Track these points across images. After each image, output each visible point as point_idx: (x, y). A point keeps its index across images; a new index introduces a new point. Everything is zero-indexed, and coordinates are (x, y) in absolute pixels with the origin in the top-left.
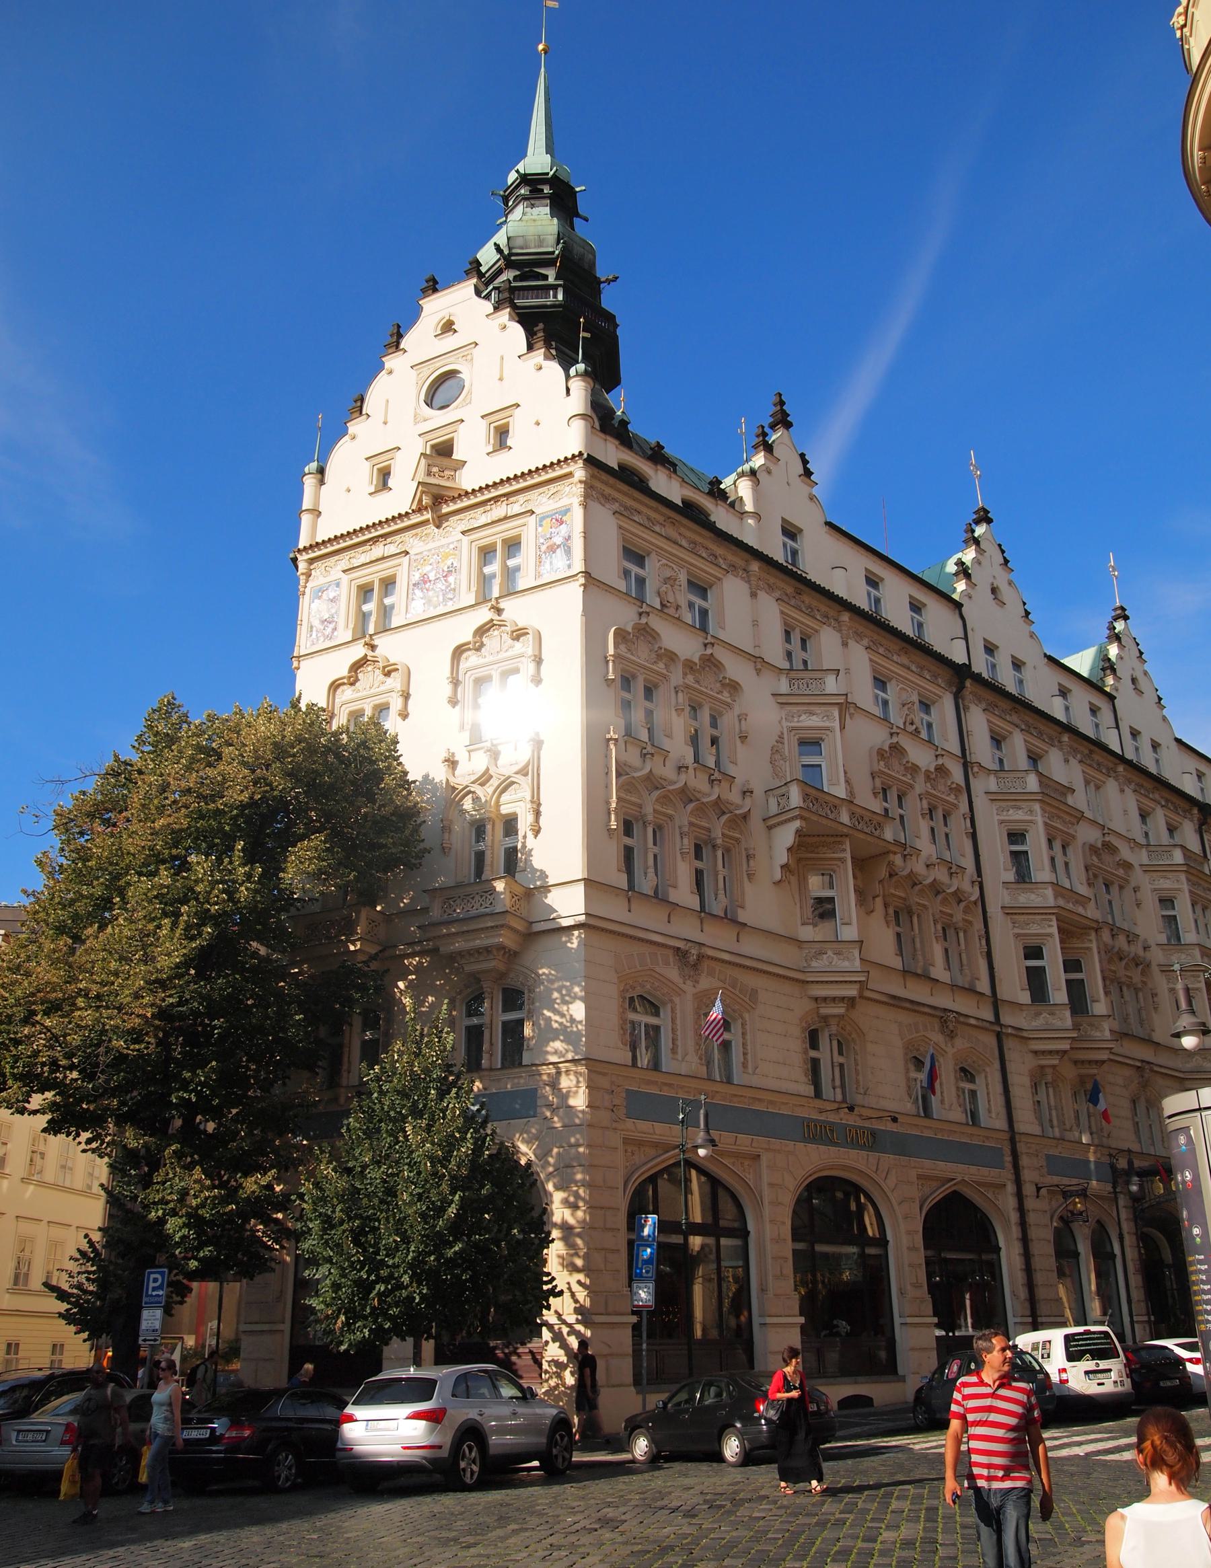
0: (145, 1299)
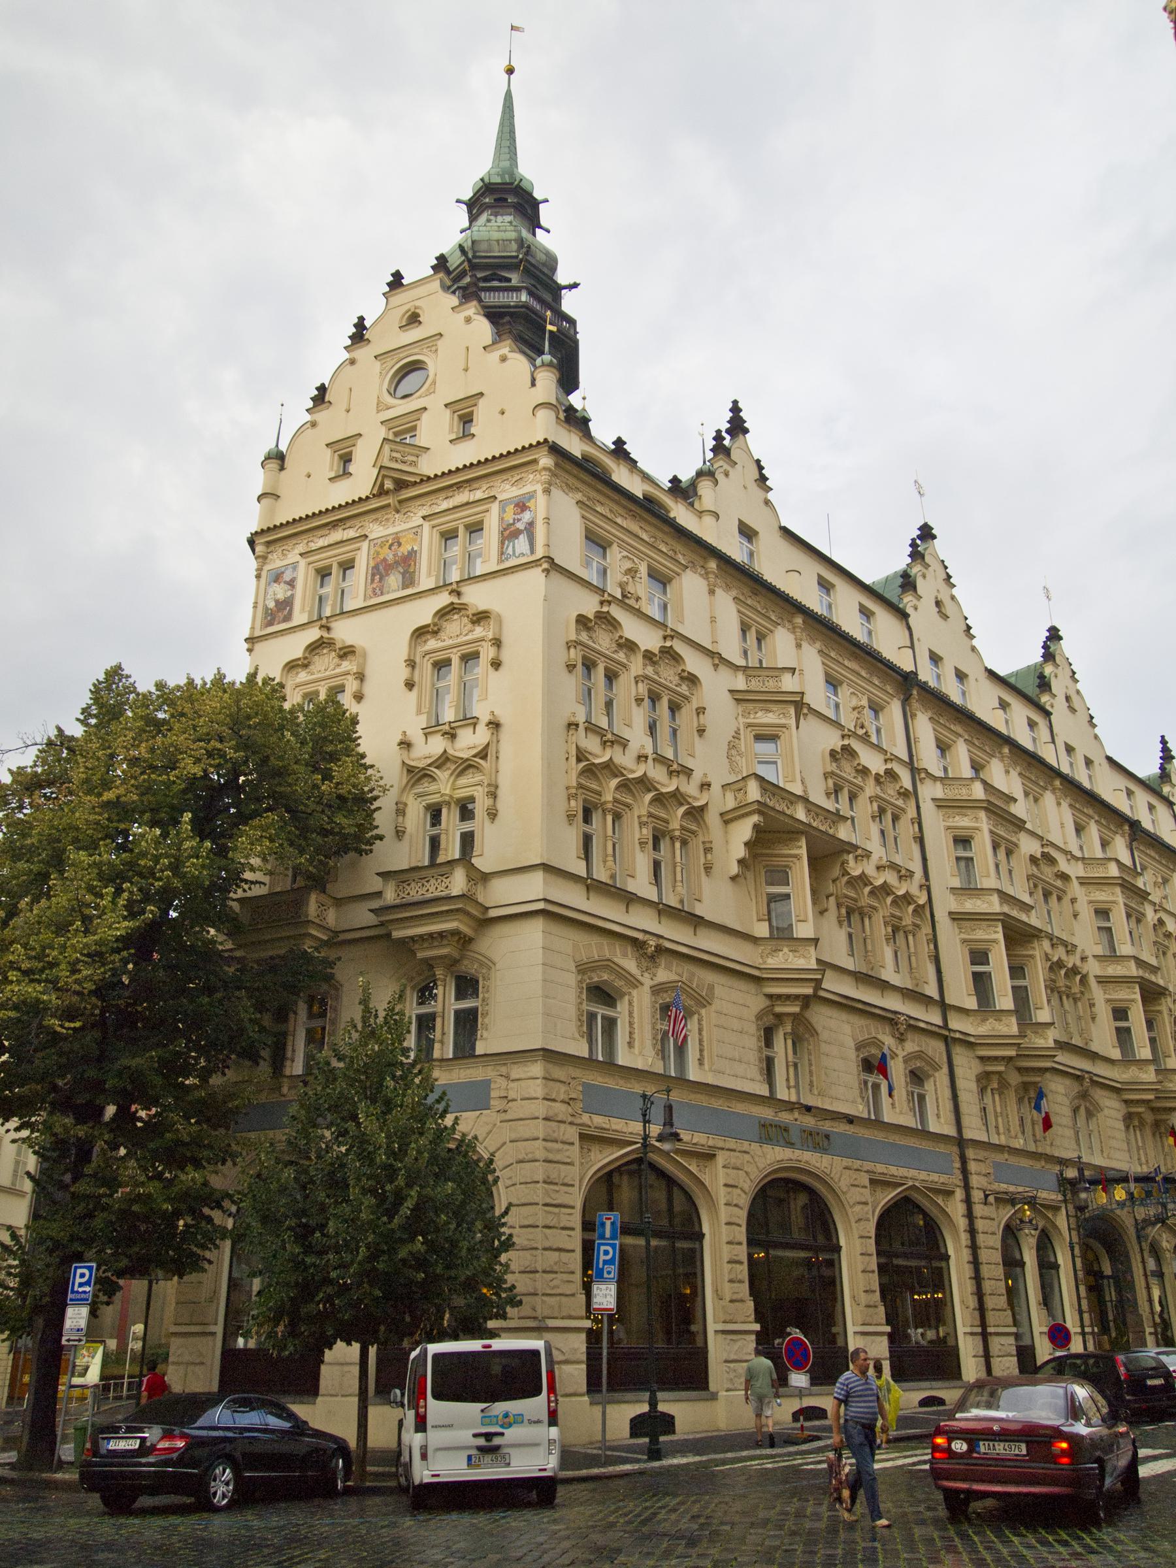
0: (70, 1296)
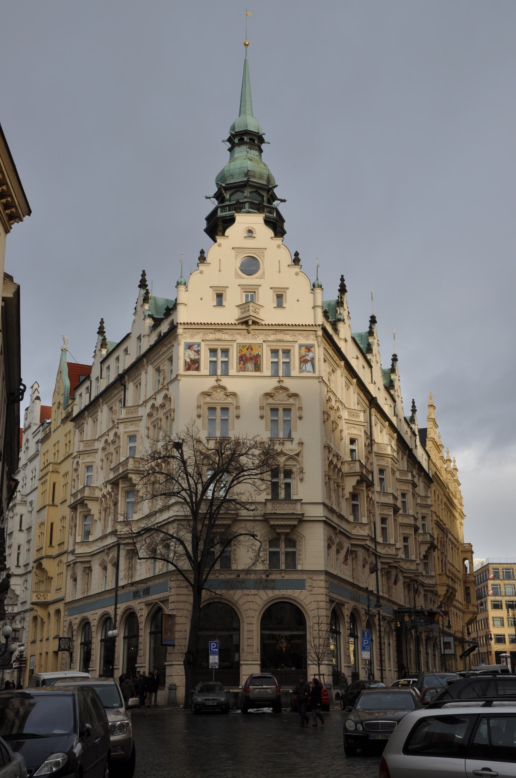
0: (210, 652)
